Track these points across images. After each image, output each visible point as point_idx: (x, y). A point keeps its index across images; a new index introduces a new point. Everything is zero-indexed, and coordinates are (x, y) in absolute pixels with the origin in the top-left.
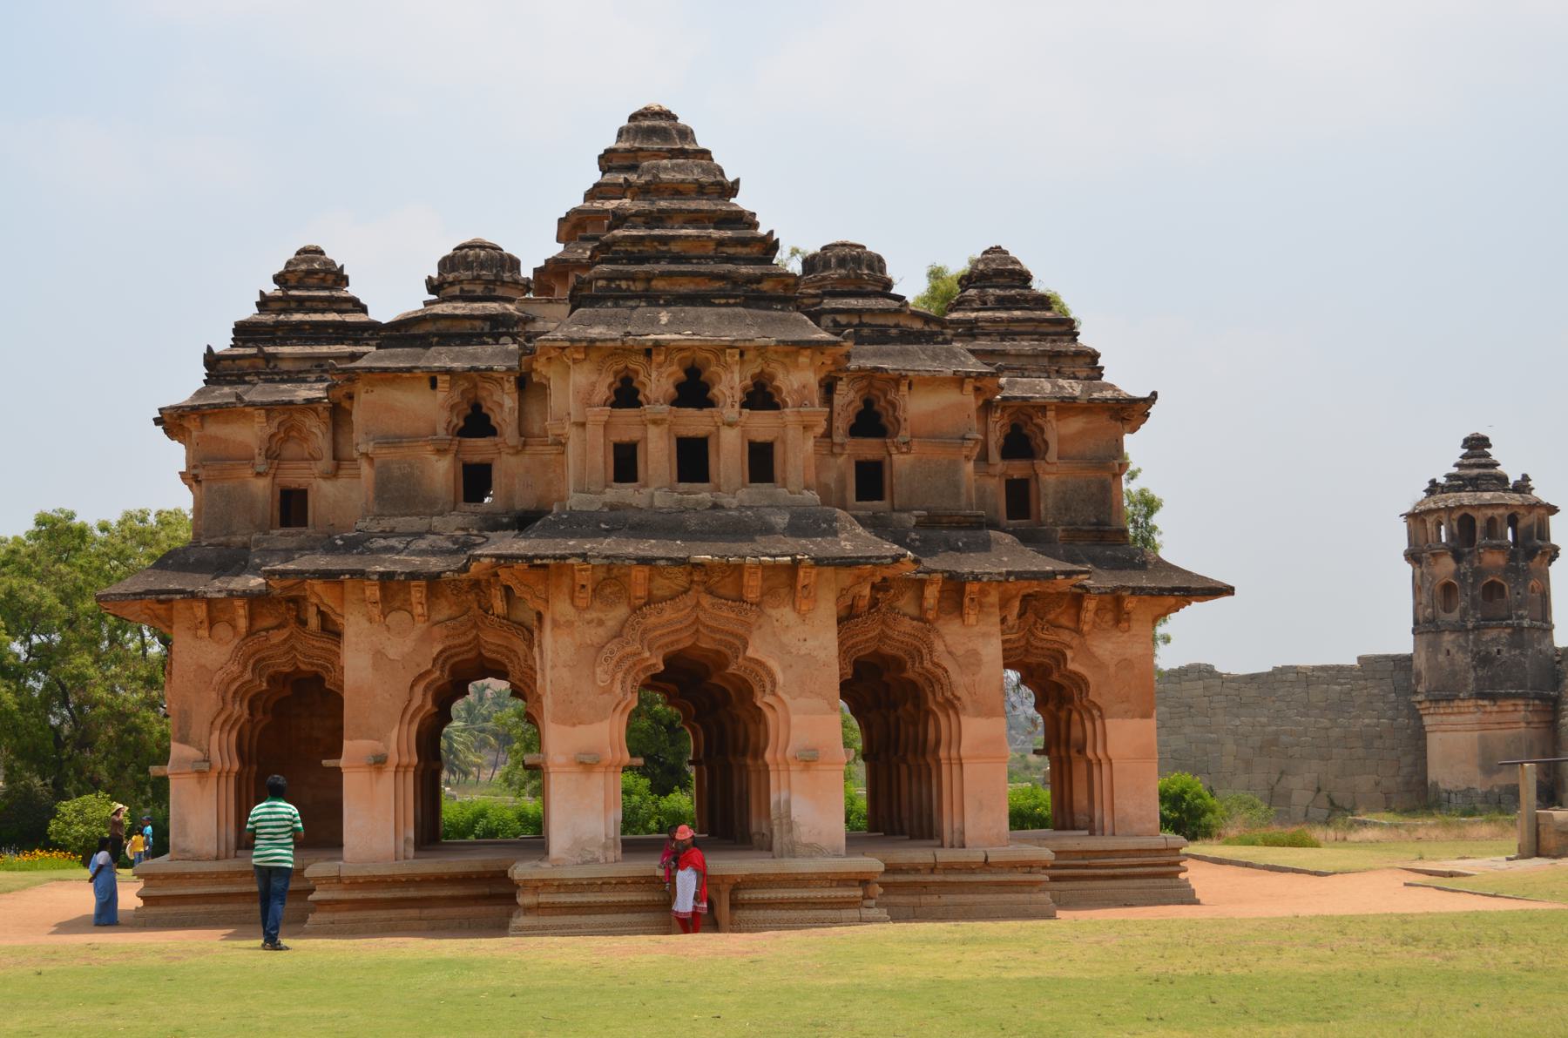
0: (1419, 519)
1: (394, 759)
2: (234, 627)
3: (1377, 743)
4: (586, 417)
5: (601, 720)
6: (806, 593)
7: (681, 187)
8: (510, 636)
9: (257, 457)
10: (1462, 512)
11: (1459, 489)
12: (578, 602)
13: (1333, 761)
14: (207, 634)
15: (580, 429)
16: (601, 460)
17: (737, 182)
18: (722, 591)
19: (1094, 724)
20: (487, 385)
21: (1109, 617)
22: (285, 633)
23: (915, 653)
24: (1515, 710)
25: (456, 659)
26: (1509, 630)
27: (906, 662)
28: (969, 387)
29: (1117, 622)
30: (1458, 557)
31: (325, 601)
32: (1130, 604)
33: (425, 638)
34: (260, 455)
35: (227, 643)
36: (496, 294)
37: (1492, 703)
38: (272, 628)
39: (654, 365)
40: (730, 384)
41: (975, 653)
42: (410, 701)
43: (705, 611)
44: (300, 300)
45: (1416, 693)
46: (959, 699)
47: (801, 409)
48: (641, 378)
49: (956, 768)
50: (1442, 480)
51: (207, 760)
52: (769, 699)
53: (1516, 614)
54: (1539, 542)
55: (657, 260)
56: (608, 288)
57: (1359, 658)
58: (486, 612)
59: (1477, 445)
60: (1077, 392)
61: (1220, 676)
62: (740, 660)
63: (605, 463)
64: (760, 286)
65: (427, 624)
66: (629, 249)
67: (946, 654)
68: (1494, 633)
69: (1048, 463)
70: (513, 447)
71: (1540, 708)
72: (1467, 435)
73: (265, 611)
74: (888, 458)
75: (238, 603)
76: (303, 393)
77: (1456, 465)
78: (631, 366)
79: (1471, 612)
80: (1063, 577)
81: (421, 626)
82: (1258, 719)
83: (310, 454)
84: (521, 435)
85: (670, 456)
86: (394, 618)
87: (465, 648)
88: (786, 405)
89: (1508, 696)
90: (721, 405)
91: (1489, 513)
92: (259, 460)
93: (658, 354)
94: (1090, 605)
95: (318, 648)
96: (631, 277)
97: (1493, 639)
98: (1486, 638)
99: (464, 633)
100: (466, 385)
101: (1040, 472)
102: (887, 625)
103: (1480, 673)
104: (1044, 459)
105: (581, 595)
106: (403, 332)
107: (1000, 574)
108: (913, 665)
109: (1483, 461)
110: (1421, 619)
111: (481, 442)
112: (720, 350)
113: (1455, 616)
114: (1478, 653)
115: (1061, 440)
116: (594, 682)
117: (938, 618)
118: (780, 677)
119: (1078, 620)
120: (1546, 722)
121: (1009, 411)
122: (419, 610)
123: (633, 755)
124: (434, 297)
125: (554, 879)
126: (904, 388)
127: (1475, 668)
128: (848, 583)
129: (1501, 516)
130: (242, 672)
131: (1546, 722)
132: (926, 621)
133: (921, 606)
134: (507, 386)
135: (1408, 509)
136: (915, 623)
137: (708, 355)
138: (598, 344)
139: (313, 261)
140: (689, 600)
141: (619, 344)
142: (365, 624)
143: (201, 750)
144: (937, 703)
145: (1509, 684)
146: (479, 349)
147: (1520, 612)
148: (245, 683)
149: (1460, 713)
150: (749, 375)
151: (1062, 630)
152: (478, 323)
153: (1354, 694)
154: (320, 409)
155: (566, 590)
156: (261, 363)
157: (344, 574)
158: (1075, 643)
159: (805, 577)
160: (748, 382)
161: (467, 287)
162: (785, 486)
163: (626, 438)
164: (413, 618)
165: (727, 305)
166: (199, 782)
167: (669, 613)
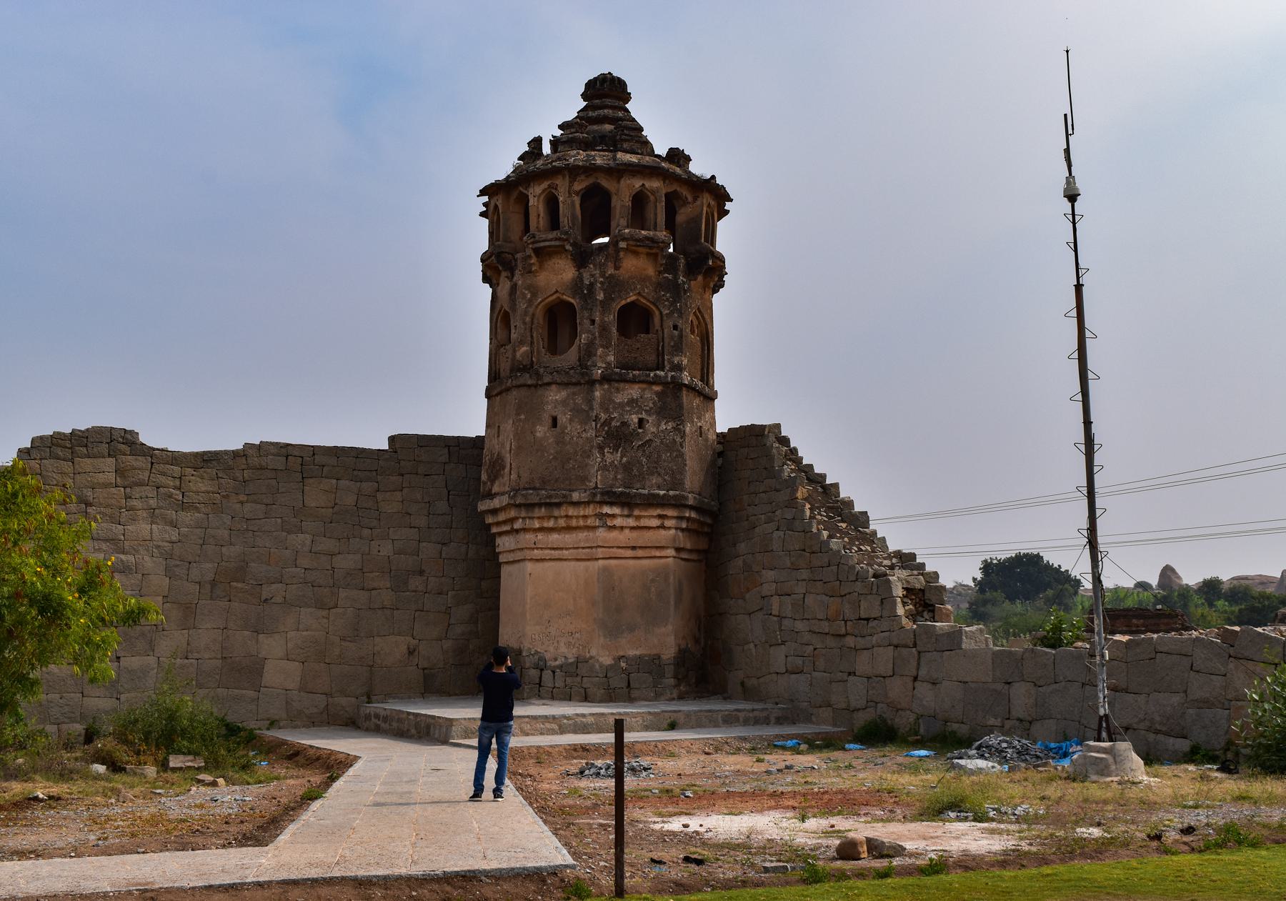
0: (515, 195)
3: (416, 582)
13: (340, 610)
24: (662, 527)
26: (657, 388)
37: (626, 512)
45: (491, 496)
53: (671, 362)
57: (392, 439)
61: (148, 452)
68: (634, 391)
71: (694, 526)
89: (652, 502)
91: (637, 183)
97: (632, 402)
98: (619, 398)
103: (609, 458)
110: (505, 366)
114: (607, 422)
127: (601, 448)
131: (698, 551)
147: (676, 360)
149: (569, 529)
153: (380, 496)
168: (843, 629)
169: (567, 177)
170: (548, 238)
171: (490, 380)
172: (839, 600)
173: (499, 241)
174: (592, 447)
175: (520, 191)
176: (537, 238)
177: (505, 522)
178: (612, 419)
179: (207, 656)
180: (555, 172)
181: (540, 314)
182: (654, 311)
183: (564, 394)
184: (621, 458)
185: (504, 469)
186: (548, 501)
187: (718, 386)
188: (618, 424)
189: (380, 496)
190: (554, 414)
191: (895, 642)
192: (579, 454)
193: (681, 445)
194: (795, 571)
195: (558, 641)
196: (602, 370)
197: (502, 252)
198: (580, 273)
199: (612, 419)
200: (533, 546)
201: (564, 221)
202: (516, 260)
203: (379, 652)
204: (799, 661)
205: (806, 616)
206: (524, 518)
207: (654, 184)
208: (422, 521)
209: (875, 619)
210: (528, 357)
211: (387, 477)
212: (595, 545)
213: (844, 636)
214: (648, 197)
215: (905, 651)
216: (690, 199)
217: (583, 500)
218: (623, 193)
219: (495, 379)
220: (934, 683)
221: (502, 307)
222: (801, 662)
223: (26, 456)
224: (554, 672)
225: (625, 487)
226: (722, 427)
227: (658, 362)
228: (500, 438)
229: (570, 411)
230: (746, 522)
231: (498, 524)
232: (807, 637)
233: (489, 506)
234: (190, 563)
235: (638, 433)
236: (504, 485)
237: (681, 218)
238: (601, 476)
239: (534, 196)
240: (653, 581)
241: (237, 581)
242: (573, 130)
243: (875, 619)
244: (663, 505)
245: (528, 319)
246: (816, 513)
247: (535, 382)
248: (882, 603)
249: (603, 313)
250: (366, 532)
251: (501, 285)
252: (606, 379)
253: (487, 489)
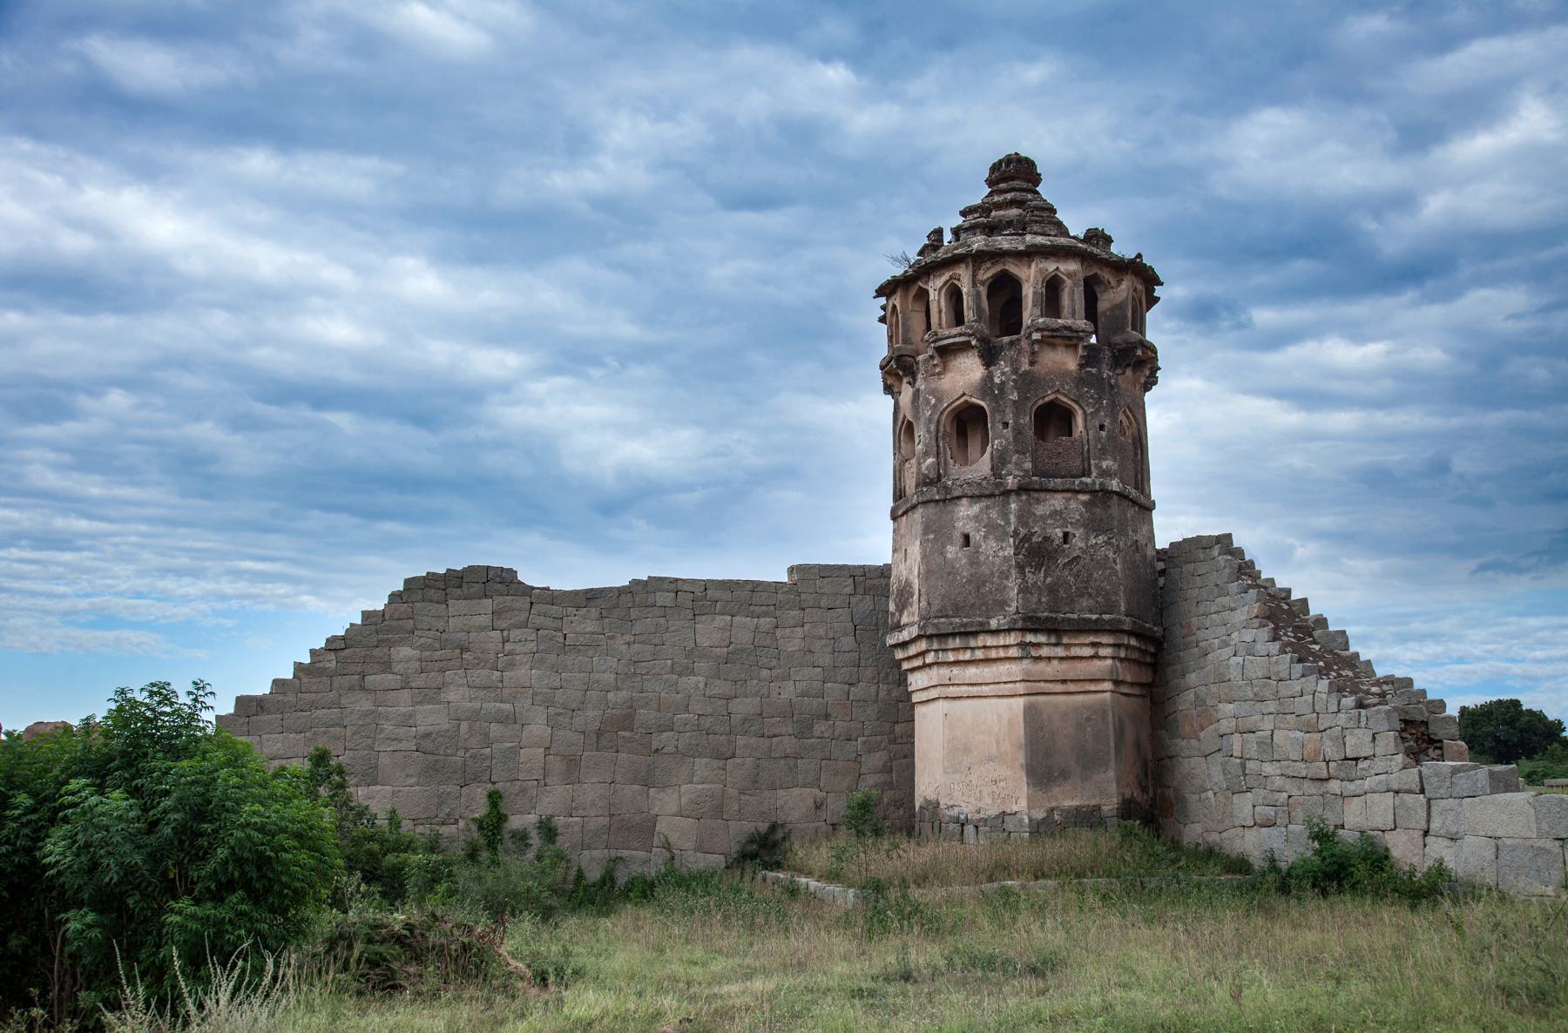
0: (914, 291)
3: (820, 728)
10: (998, 268)
13: (738, 761)
24: (1096, 657)
26: (1084, 497)
30: (989, 356)
37: (1053, 640)
45: (898, 627)
53: (1098, 467)
57: (791, 570)
68: (1057, 502)
71: (1135, 655)
79: (1015, 458)
82: (596, 676)
89: (1082, 628)
91: (1051, 266)
97: (1055, 513)
98: (1040, 510)
113: (981, 467)
114: (1027, 538)
120: (1141, 685)
127: (1021, 568)
129: (1069, 275)
131: (1141, 685)
145: (1085, 602)
147: (1104, 464)
153: (779, 633)
168: (1325, 772)
169: (971, 264)
170: (952, 334)
171: (895, 500)
172: (1319, 735)
173: (897, 343)
175: (920, 287)
176: (939, 336)
177: (916, 656)
178: (1033, 534)
179: (592, 814)
180: (955, 261)
182: (1075, 410)
183: (976, 508)
184: (1045, 577)
185: (912, 597)
186: (963, 630)
187: (1156, 491)
188: (1040, 539)
189: (779, 633)
190: (966, 531)
191: (1395, 787)
192: (996, 575)
193: (1115, 562)
194: (1259, 703)
195: (980, 791)
196: (1019, 478)
197: (902, 356)
198: (989, 372)
199: (1033, 534)
200: (948, 682)
201: (969, 315)
202: (917, 363)
203: (782, 807)
204: (1270, 811)
205: (1276, 757)
206: (936, 651)
207: (1072, 266)
208: (826, 660)
209: (1366, 758)
210: (934, 469)
211: (787, 612)
212: (1019, 679)
213: (1327, 780)
214: (1063, 281)
215: (1409, 798)
216: (1113, 282)
217: (1002, 628)
218: (1030, 278)
219: (901, 498)
220: (1452, 839)
221: (905, 417)
222: (1273, 814)
223: (398, 599)
224: (977, 827)
225: (1051, 612)
226: (1162, 541)
227: (1084, 468)
228: (908, 562)
229: (984, 527)
230: (1196, 649)
231: (909, 658)
232: (1279, 782)
233: (898, 639)
234: (573, 711)
235: (1064, 550)
236: (913, 614)
237: (1103, 305)
238: (1023, 599)
239: (935, 290)
240: (1088, 719)
241: (625, 730)
242: (975, 215)
243: (1366, 758)
244: (1096, 632)
245: (933, 427)
246: (1281, 633)
247: (943, 497)
248: (1374, 738)
249: (1017, 416)
250: (765, 673)
251: (902, 395)
252: (1022, 489)
253: (895, 621)
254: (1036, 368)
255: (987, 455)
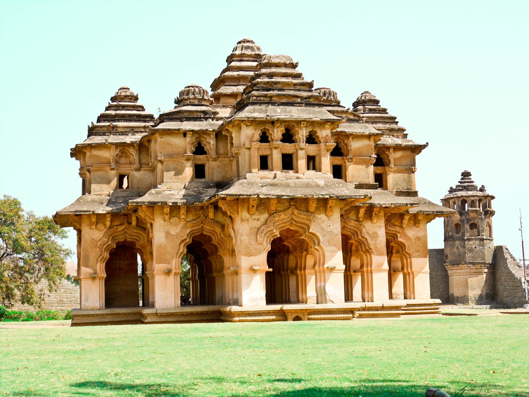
1: (174, 271)
2: (105, 225)
4: (251, 145)
5: (260, 254)
6: (330, 209)
7: (278, 65)
8: (215, 226)
9: (112, 162)
11: (462, 190)
12: (250, 212)
14: (94, 227)
15: (248, 150)
16: (257, 161)
17: (297, 63)
18: (301, 209)
19: (407, 260)
20: (204, 136)
21: (412, 222)
22: (123, 227)
23: (355, 233)
24: (481, 268)
25: (195, 235)
27: (351, 236)
28: (372, 139)
29: (415, 224)
31: (147, 214)
32: (420, 218)
33: (184, 227)
34: (113, 162)
35: (102, 231)
36: (202, 103)
38: (119, 225)
39: (275, 127)
40: (302, 133)
41: (376, 233)
42: (179, 250)
43: (295, 215)
44: (124, 107)
45: (445, 262)
46: (371, 249)
47: (327, 144)
48: (270, 132)
49: (369, 274)
50: (454, 187)
51: (95, 273)
52: (316, 247)
54: (489, 209)
55: (273, 90)
56: (256, 100)
58: (206, 217)
59: (466, 175)
60: (400, 143)
62: (307, 233)
63: (258, 162)
64: (310, 100)
65: (185, 222)
66: (263, 86)
67: (366, 234)
69: (390, 168)
70: (214, 158)
72: (463, 171)
73: (115, 219)
74: (344, 164)
75: (108, 216)
76: (129, 139)
77: (459, 182)
78: (267, 128)
80: (410, 205)
81: (183, 223)
83: (130, 162)
84: (217, 154)
85: (280, 160)
86: (173, 220)
87: (198, 231)
88: (320, 142)
90: (298, 142)
91: (472, 198)
92: (113, 164)
93: (278, 123)
94: (407, 217)
95: (135, 232)
96: (265, 96)
99: (198, 225)
100: (197, 136)
101: (387, 170)
102: (346, 223)
103: (469, 255)
104: (388, 166)
105: (252, 210)
106: (165, 117)
107: (389, 204)
108: (354, 237)
109: (469, 180)
111: (202, 157)
112: (299, 122)
115: (395, 159)
116: (257, 240)
117: (363, 221)
118: (321, 239)
119: (402, 223)
120: (491, 272)
121: (377, 149)
122: (183, 217)
123: (269, 268)
124: (177, 105)
125: (245, 311)
126: (351, 139)
128: (343, 206)
129: (476, 200)
130: (108, 241)
131: (491, 272)
132: (359, 221)
133: (357, 216)
134: (212, 136)
135: (443, 197)
136: (356, 222)
137: (294, 124)
138: (257, 119)
139: (126, 92)
140: (290, 211)
141: (265, 119)
142: (163, 222)
143: (93, 270)
144: (363, 251)
146: (201, 122)
147: (482, 234)
148: (108, 245)
149: (461, 269)
150: (308, 131)
151: (396, 227)
152: (199, 114)
154: (135, 145)
155: (246, 208)
156: (111, 129)
157: (159, 203)
158: (401, 231)
159: (331, 203)
160: (308, 134)
161: (192, 101)
162: (320, 171)
163: (265, 154)
164: (180, 220)
165: (299, 106)
166: (93, 281)
167: (283, 216)
174: (465, 253)
181: (454, 226)
204: (508, 295)
231: (448, 268)
232: (509, 290)
240: (480, 279)
245: (451, 227)
254: (470, 217)
255: (461, 233)
